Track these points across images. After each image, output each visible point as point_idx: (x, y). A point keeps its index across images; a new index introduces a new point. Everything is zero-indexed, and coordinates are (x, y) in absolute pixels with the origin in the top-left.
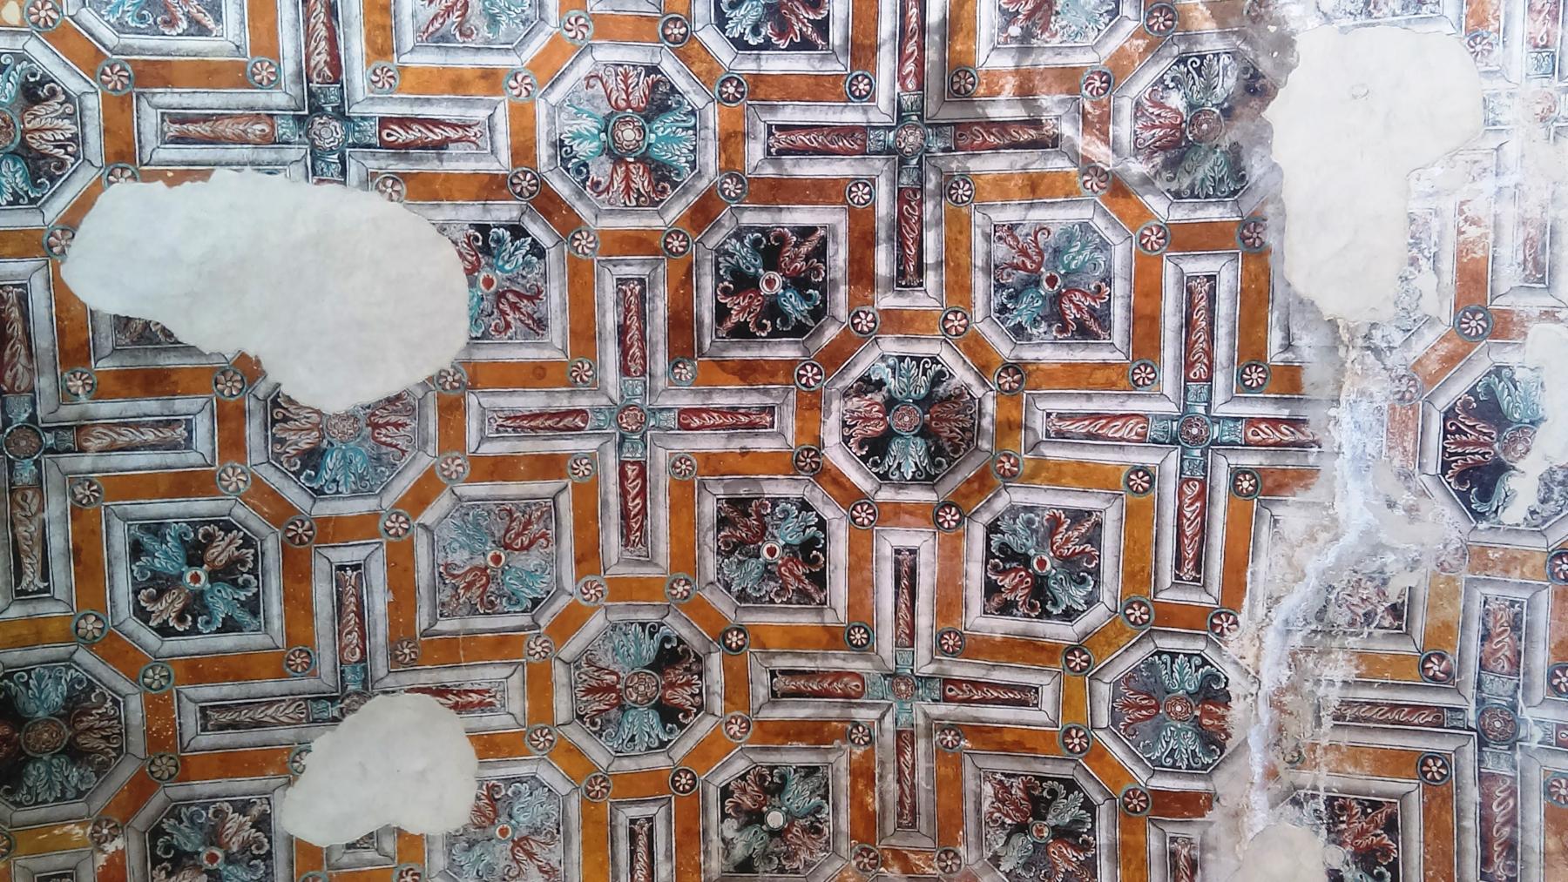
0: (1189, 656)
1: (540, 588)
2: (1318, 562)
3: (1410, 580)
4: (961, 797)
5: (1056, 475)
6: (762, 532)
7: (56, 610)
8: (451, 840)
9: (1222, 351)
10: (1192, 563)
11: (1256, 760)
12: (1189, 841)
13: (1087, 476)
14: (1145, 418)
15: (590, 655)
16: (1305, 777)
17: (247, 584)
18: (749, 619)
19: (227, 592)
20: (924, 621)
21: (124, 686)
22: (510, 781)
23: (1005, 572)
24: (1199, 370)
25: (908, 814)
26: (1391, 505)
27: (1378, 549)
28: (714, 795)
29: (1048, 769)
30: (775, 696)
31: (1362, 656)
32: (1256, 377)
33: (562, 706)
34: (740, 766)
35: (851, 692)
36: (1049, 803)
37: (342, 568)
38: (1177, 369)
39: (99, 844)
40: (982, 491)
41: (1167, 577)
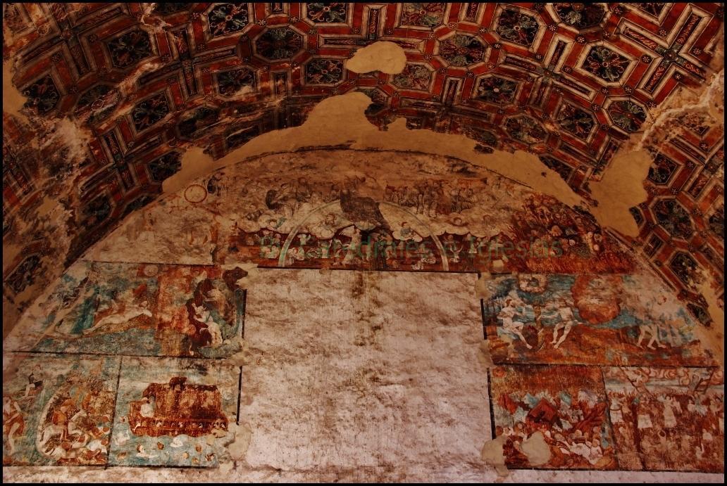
0: (638, 106)
1: (436, 22)
2: (685, 106)
3: (710, 125)
4: (556, 104)
5: (621, 45)
6: (516, 22)
7: (285, 16)
8: (395, 76)
9: (691, 39)
10: (652, 86)
11: (645, 137)
12: (616, 143)
13: (630, 50)
14: (657, 44)
15: (447, 41)
16: (656, 147)
17: (342, 12)
18: (503, 42)
19: (336, 13)
20: (561, 62)
21: (303, 34)
22: (415, 65)
23: (593, 61)
24: (681, 40)
25: (538, 101)
26: (716, 105)
27: (706, 113)
28: (479, 80)
29: (584, 110)
30: (506, 63)
31: (686, 132)
32: (698, 52)
33: (436, 51)
34: (489, 76)
35: (531, 68)
36: (580, 117)
37: (373, 10)
38: (675, 36)
39: (293, 68)
40: (594, 38)
41: (642, 86)
